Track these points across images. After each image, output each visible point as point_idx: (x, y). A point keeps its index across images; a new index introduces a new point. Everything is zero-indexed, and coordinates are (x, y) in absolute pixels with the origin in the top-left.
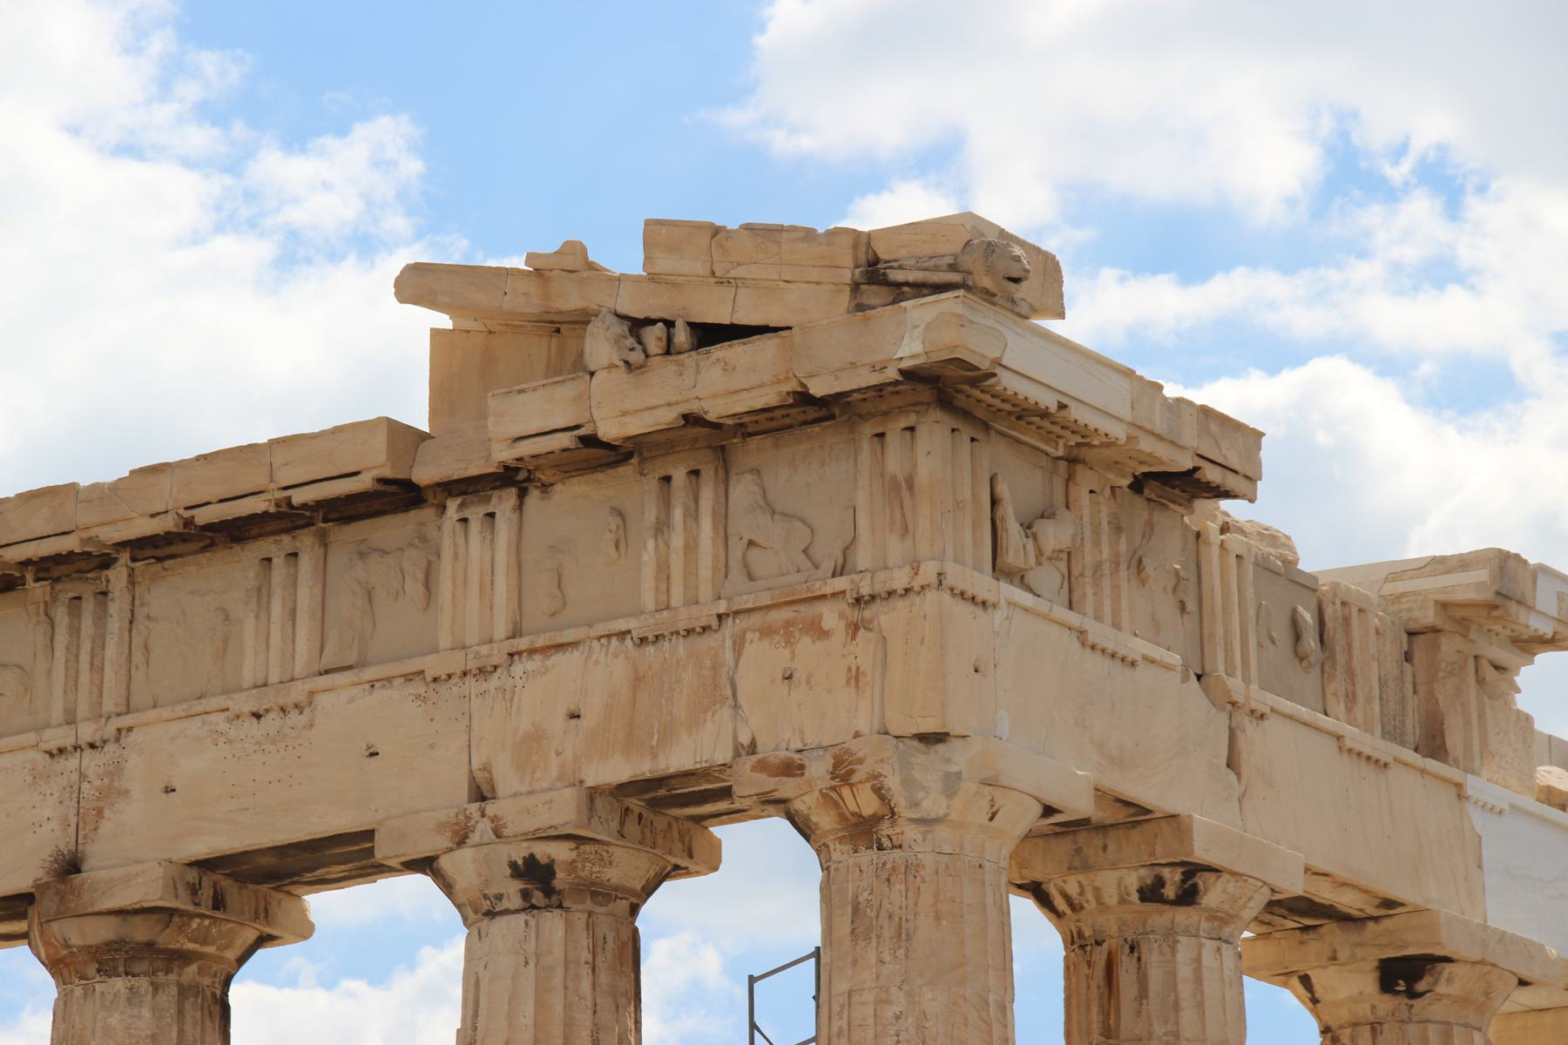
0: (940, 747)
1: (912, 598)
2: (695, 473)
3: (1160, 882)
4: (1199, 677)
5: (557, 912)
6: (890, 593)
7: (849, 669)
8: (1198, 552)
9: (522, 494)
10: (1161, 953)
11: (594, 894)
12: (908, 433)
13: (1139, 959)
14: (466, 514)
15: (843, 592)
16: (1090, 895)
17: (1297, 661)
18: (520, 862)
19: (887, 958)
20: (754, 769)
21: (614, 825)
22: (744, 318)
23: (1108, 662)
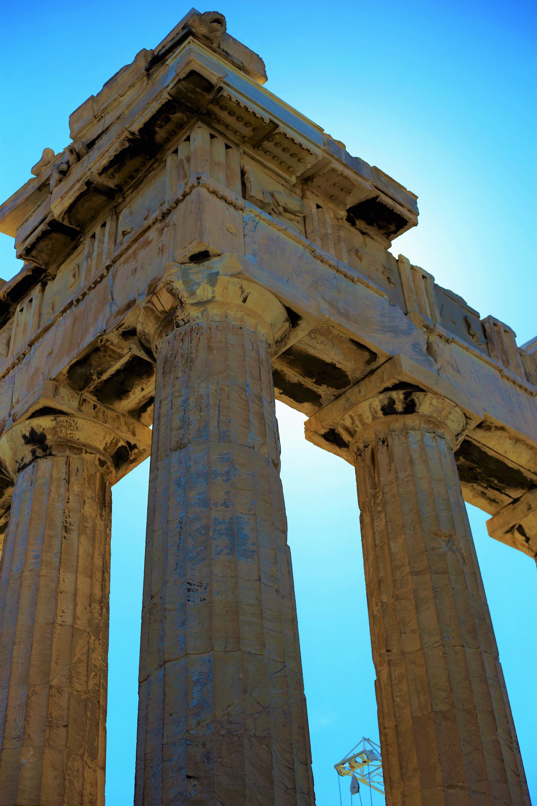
0: (206, 263)
1: (188, 198)
2: (104, 225)
3: (392, 402)
4: (406, 315)
5: (49, 457)
6: (177, 202)
7: (159, 248)
8: (398, 267)
9: (44, 285)
10: (399, 440)
11: (72, 448)
12: (187, 142)
13: (388, 445)
14: (23, 306)
15: (157, 220)
16: (357, 422)
17: (471, 337)
18: (28, 435)
19: (180, 374)
20: (115, 317)
21: (75, 404)
22: (106, 126)
23: (333, 272)
